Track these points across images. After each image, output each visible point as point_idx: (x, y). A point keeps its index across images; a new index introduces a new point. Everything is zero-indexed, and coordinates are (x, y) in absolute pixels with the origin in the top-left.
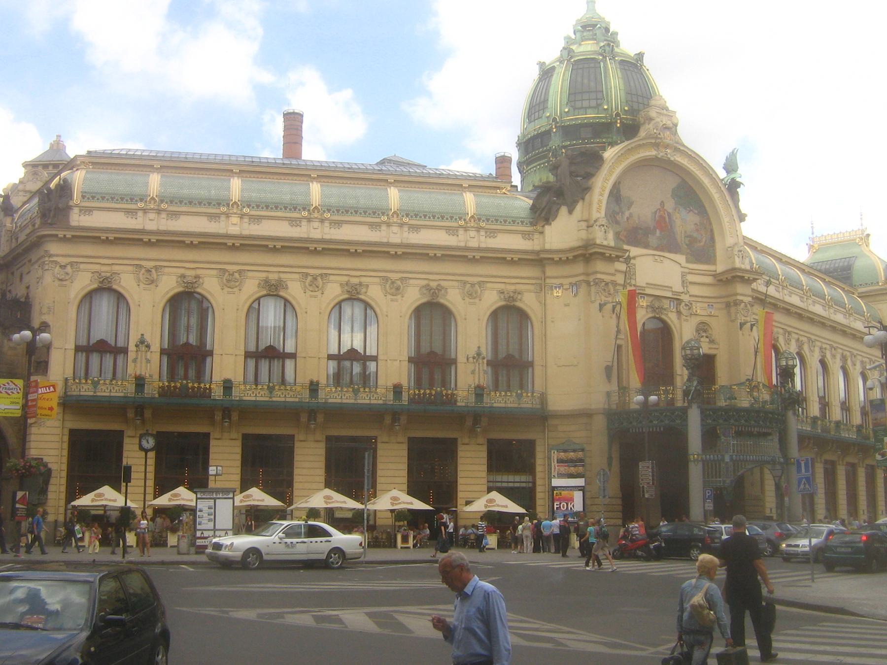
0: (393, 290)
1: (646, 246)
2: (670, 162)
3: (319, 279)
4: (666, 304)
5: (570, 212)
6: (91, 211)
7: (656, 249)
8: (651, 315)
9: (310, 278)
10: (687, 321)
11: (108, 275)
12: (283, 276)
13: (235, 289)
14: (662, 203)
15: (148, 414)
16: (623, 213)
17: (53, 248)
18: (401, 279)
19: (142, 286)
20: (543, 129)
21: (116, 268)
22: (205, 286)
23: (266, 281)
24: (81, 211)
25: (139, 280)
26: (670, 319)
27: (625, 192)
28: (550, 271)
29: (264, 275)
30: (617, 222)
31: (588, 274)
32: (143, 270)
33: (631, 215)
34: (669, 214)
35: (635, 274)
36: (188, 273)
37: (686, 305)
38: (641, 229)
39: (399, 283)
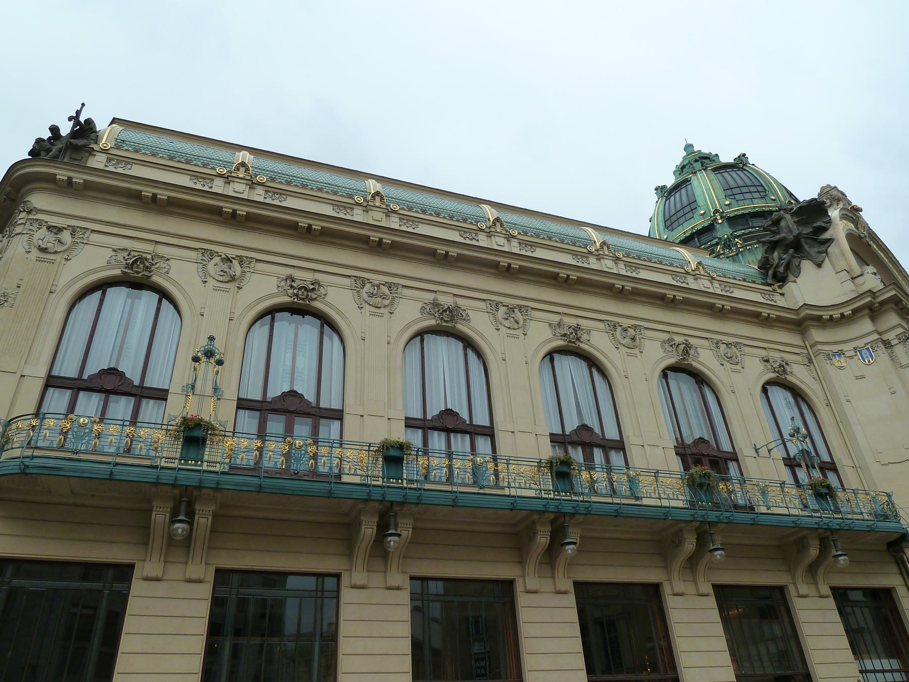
0: (627, 341)
3: (516, 311)
5: (819, 265)
6: (128, 163)
9: (503, 310)
11: (149, 257)
12: (460, 302)
15: (204, 520)
17: (38, 200)
18: (635, 327)
19: (211, 283)
20: (699, 227)
21: (162, 250)
23: (435, 304)
24: (109, 160)
25: (206, 273)
28: (817, 335)
29: (430, 297)
31: (880, 334)
36: (297, 274)
39: (631, 332)
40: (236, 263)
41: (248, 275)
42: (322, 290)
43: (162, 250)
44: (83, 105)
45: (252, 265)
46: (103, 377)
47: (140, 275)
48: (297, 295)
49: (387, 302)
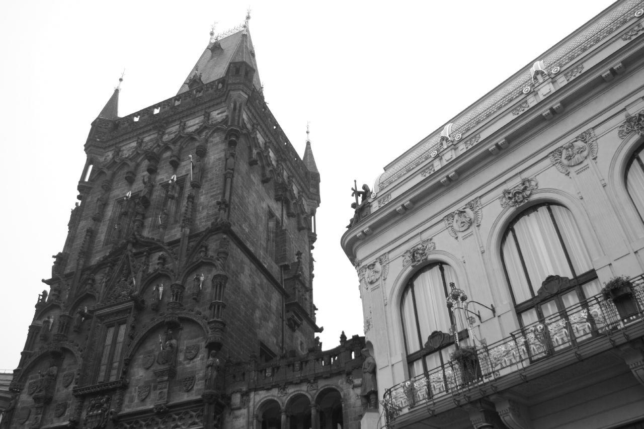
6: (389, 195)
11: (420, 246)
13: (588, 161)
19: (460, 235)
21: (425, 236)
22: (541, 186)
29: (622, 118)
32: (456, 217)
36: (510, 186)
40: (468, 210)
41: (480, 212)
42: (533, 183)
43: (425, 236)
44: (355, 181)
45: (479, 203)
46: (432, 341)
47: (421, 262)
48: (516, 202)
49: (585, 154)
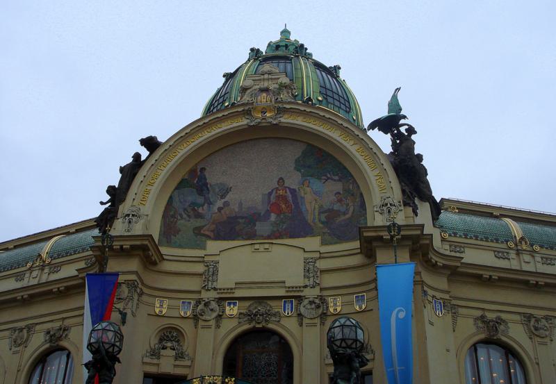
1: (251, 236)
2: (277, 127)
4: (277, 306)
7: (269, 237)
8: (246, 327)
10: (315, 325)
14: (281, 180)
16: (210, 203)
26: (283, 327)
27: (214, 177)
30: (199, 216)
33: (226, 204)
34: (293, 191)
35: (215, 273)
37: (311, 303)
38: (242, 218)
